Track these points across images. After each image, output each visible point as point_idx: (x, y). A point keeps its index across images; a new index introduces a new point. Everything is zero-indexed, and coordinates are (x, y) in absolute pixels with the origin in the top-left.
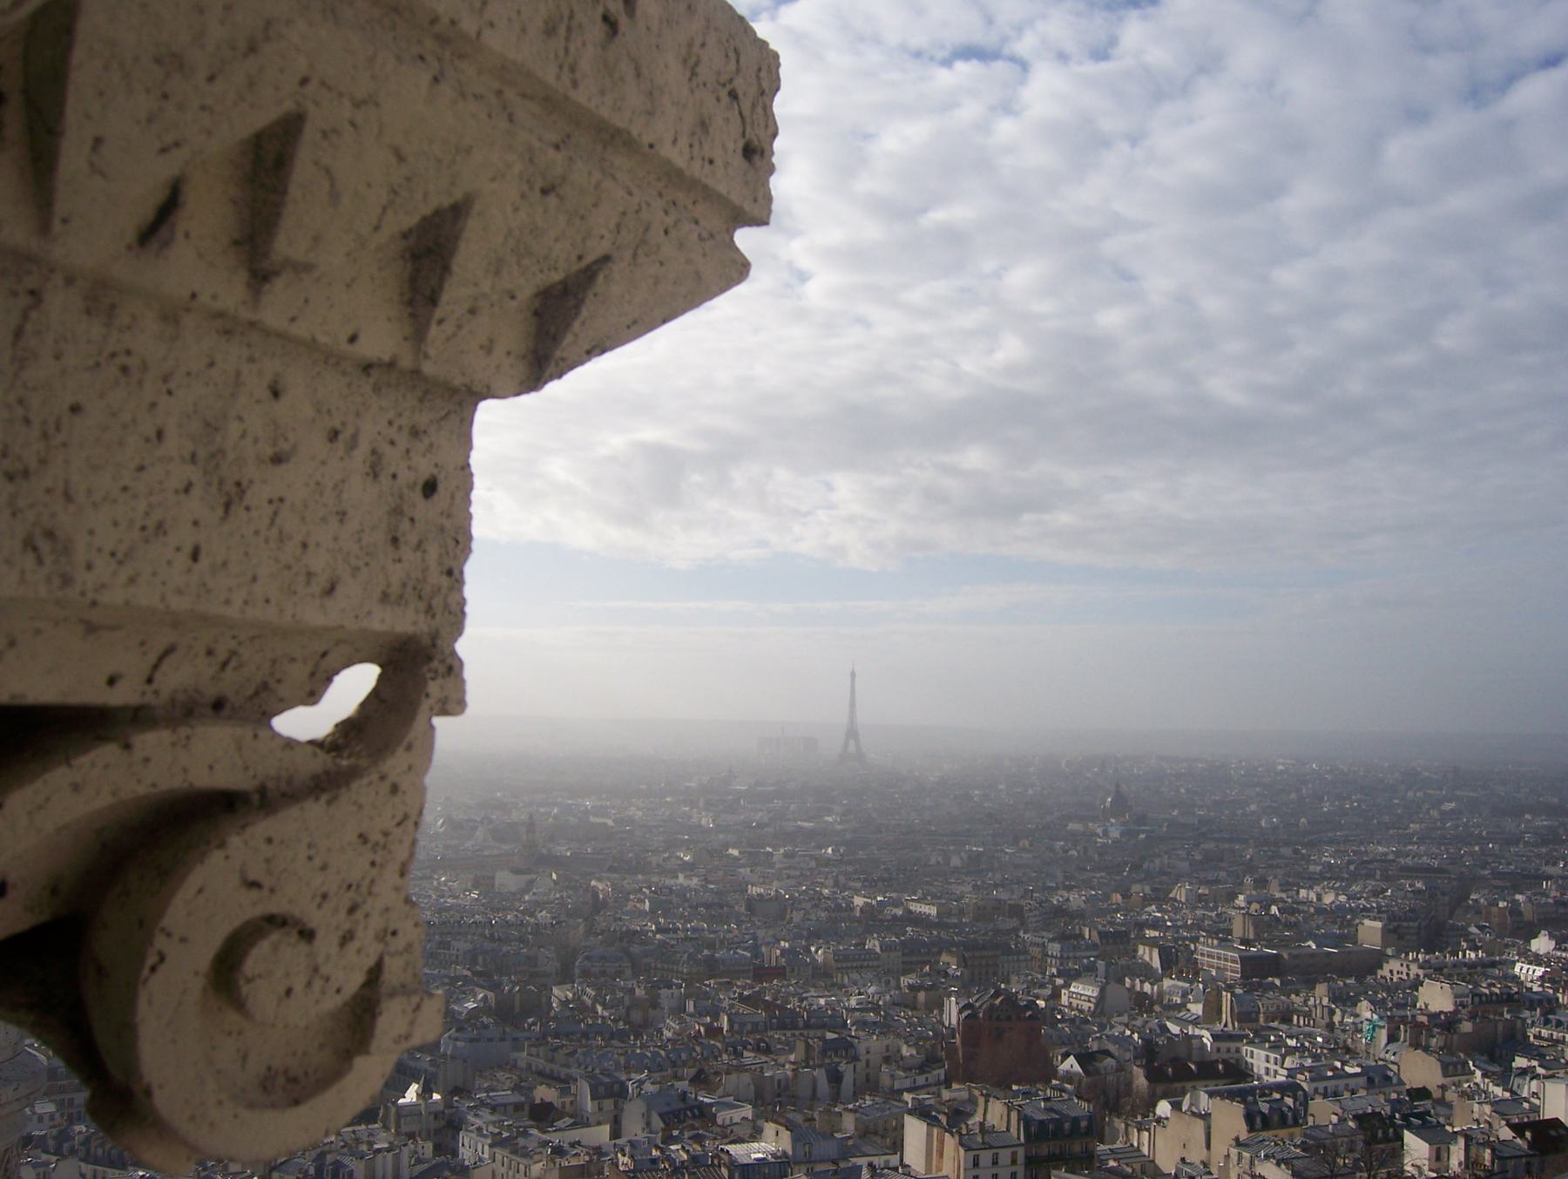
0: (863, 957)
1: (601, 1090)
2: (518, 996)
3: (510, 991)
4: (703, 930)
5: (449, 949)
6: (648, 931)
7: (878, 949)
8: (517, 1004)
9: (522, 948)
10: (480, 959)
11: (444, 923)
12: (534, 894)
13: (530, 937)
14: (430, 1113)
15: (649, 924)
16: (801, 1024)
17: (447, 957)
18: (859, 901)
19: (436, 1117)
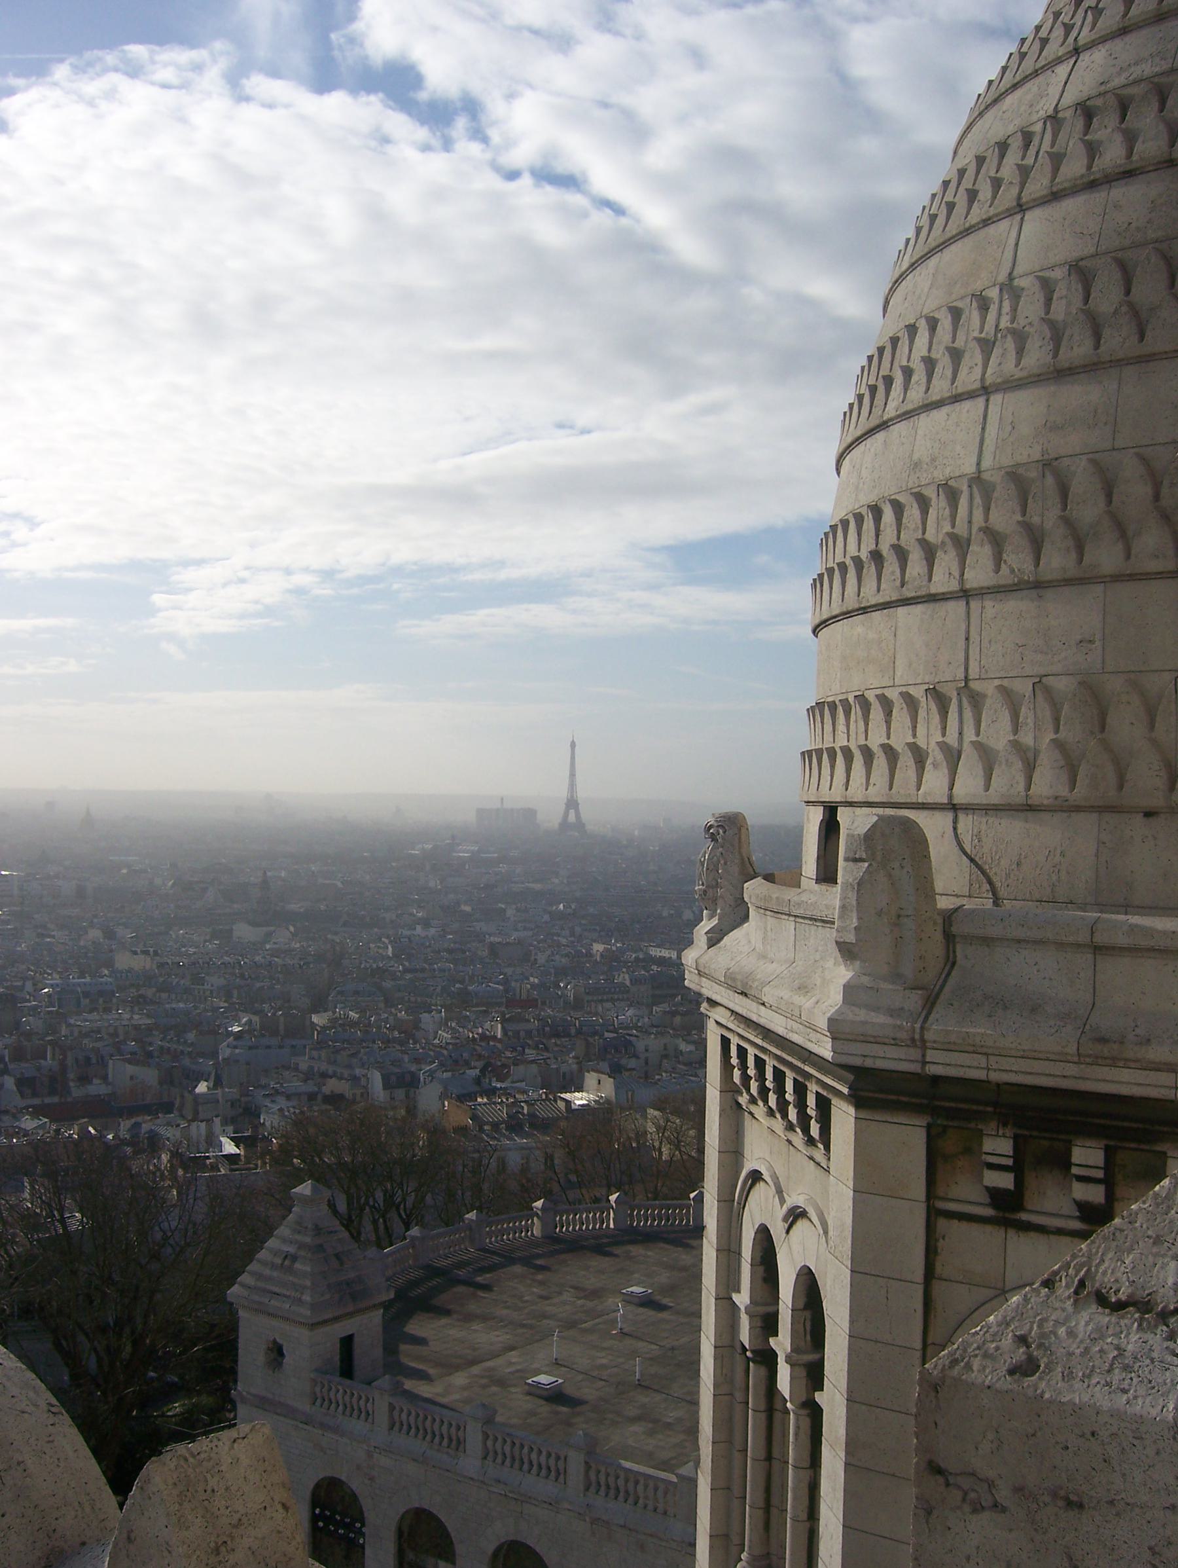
0: (613, 990)
1: (393, 1079)
2: (282, 1019)
3: (274, 1014)
4: (450, 970)
5: (203, 985)
6: (395, 972)
7: (628, 983)
8: (281, 1028)
9: (275, 984)
10: (235, 993)
11: (194, 964)
12: (275, 943)
13: (280, 976)
14: (227, 1101)
15: (396, 965)
16: (573, 1031)
17: (201, 992)
18: (598, 947)
19: (232, 1105)
